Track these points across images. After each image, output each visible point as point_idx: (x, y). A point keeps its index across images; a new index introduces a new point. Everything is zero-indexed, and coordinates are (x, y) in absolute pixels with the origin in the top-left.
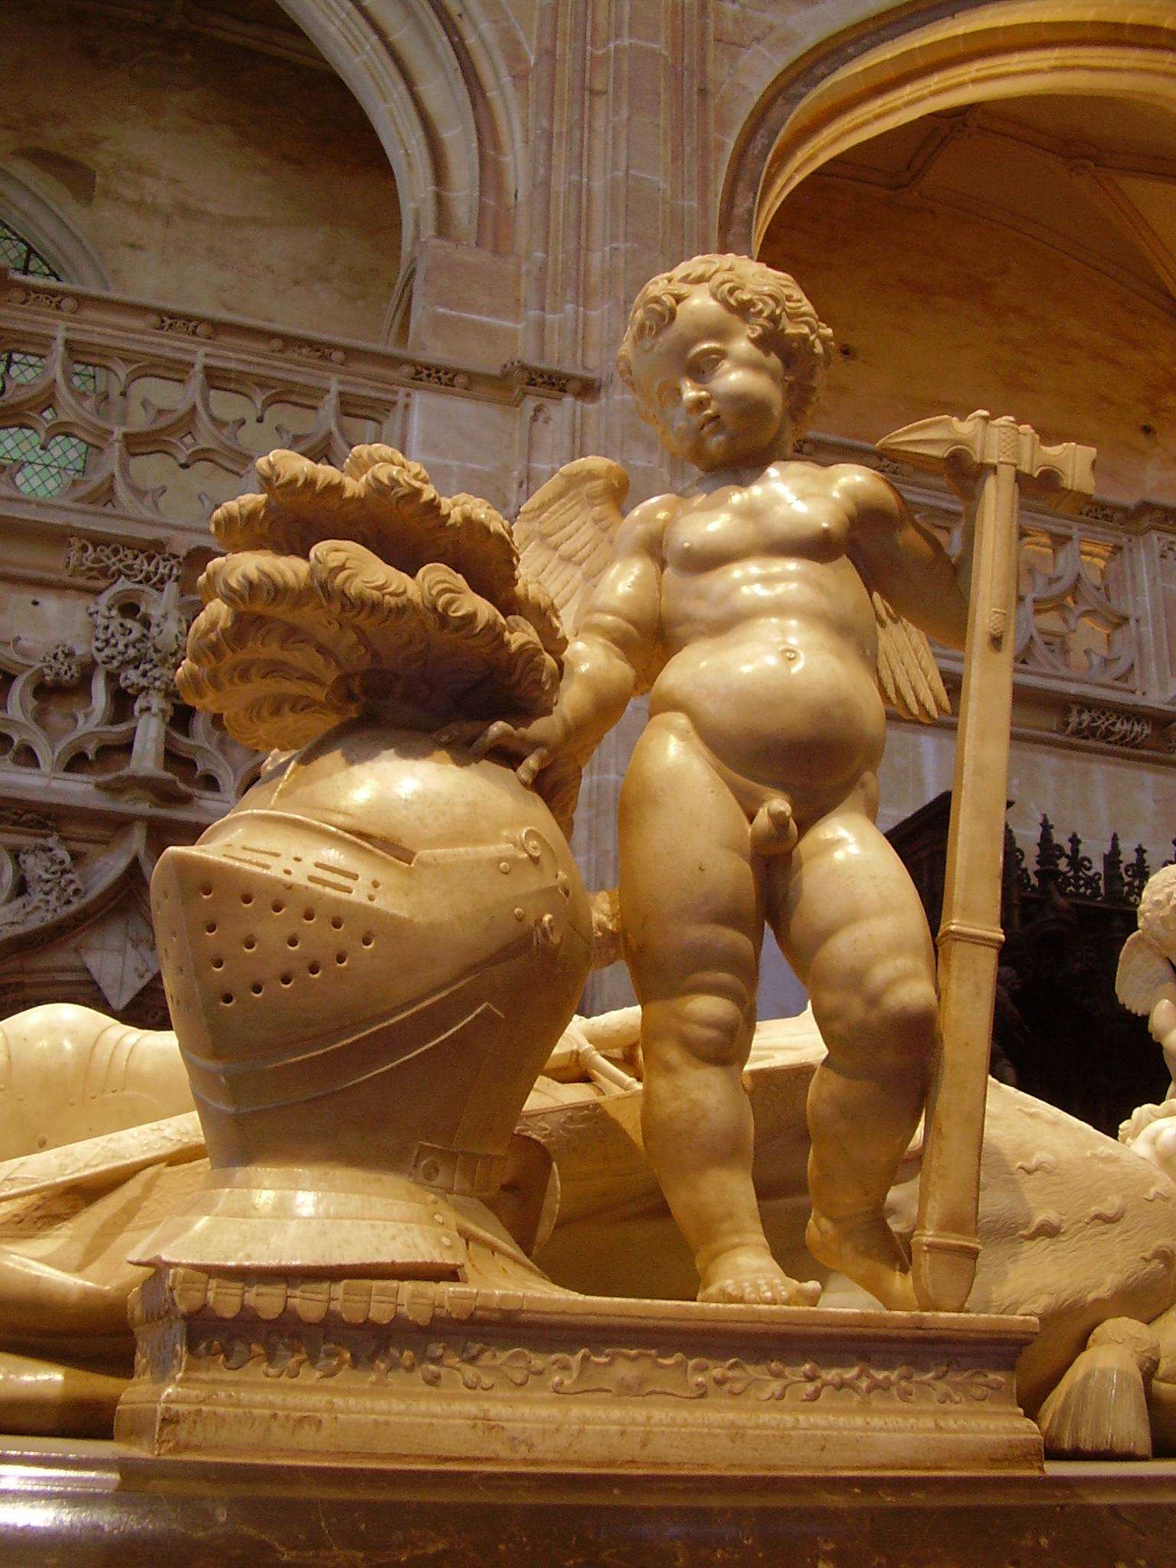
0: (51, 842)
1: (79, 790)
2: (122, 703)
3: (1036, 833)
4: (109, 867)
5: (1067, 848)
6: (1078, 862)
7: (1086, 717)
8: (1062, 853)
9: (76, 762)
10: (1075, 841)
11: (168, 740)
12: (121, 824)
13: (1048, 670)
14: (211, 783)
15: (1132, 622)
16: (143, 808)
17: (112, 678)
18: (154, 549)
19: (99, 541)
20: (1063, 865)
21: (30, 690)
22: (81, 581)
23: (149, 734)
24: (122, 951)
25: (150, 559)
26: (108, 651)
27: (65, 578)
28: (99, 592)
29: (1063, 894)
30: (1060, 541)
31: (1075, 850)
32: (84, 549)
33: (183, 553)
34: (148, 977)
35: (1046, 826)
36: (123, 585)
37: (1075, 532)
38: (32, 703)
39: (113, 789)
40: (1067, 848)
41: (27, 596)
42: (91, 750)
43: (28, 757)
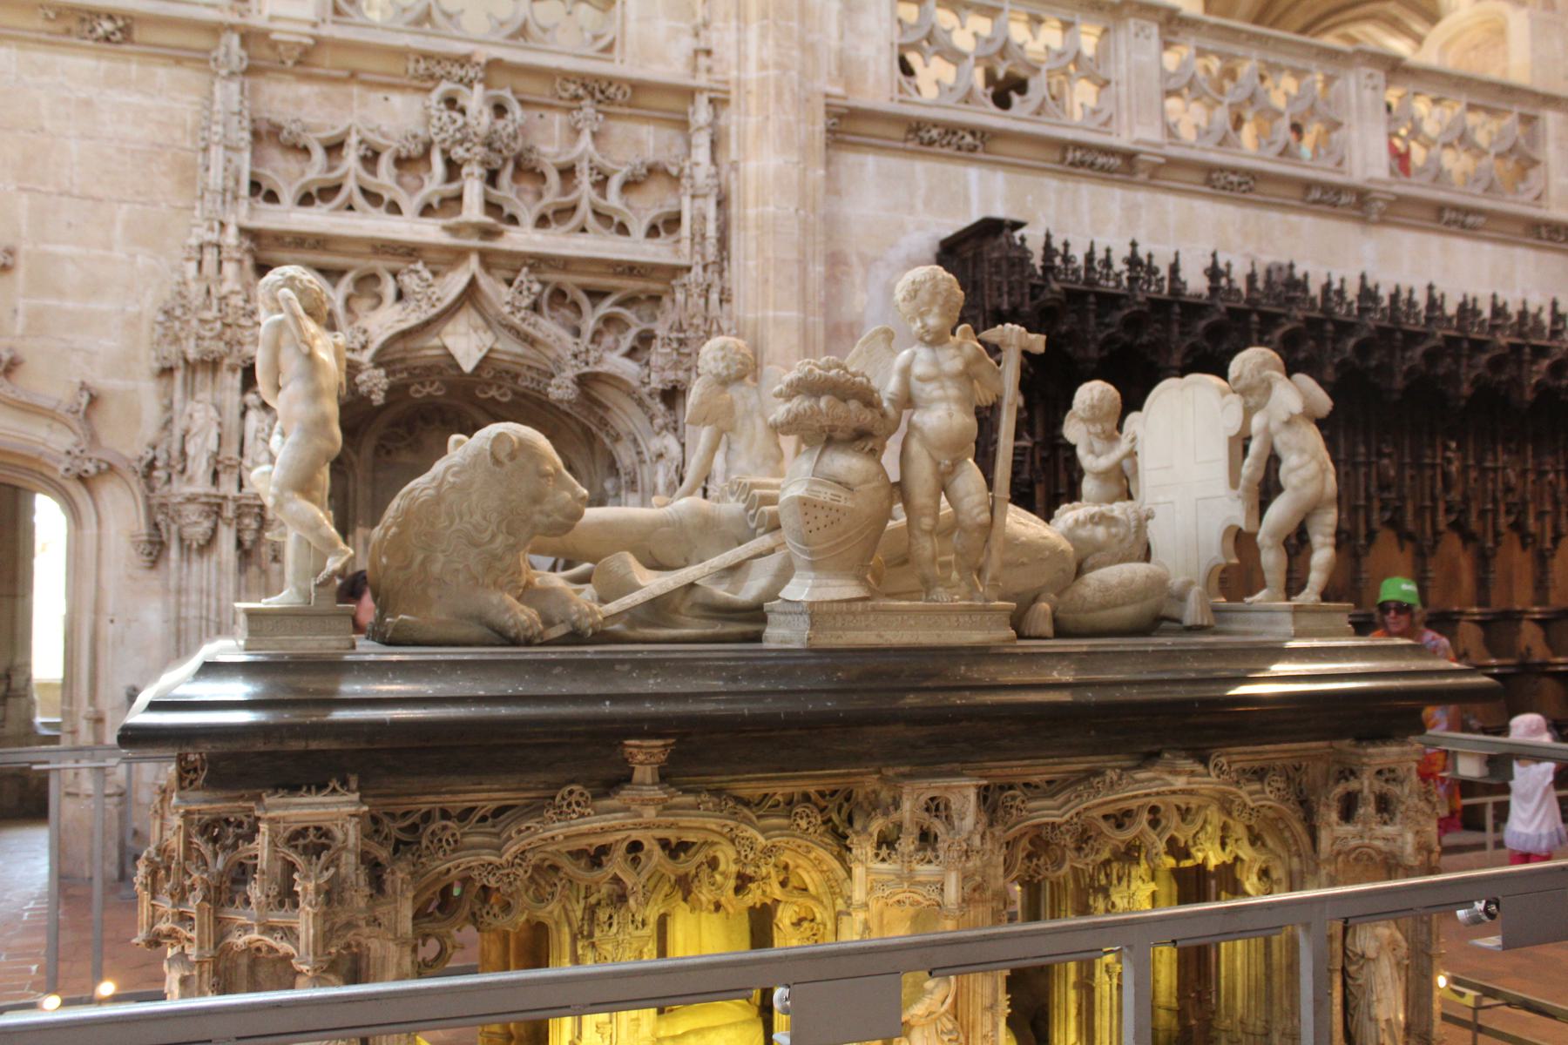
0: (419, 266)
1: (430, 231)
2: (453, 169)
3: (1041, 242)
4: (455, 282)
5: (1061, 249)
6: (1067, 259)
7: (1078, 154)
8: (1056, 252)
9: (427, 210)
10: (1066, 245)
11: (486, 193)
12: (460, 255)
13: (1053, 120)
14: (513, 220)
15: (1113, 84)
16: (475, 242)
17: (445, 152)
18: (464, 60)
19: (427, 56)
20: (1058, 261)
21: (391, 162)
22: (416, 83)
23: (473, 190)
24: (467, 334)
25: (462, 66)
26: (443, 135)
27: (405, 81)
28: (429, 91)
29: (1056, 280)
30: (1067, 26)
31: (1066, 251)
32: (418, 61)
33: (483, 60)
34: (485, 351)
35: (1048, 236)
36: (445, 86)
37: (1077, 18)
38: (394, 171)
39: (453, 230)
40: (1061, 249)
41: (380, 95)
42: (435, 202)
43: (394, 208)
